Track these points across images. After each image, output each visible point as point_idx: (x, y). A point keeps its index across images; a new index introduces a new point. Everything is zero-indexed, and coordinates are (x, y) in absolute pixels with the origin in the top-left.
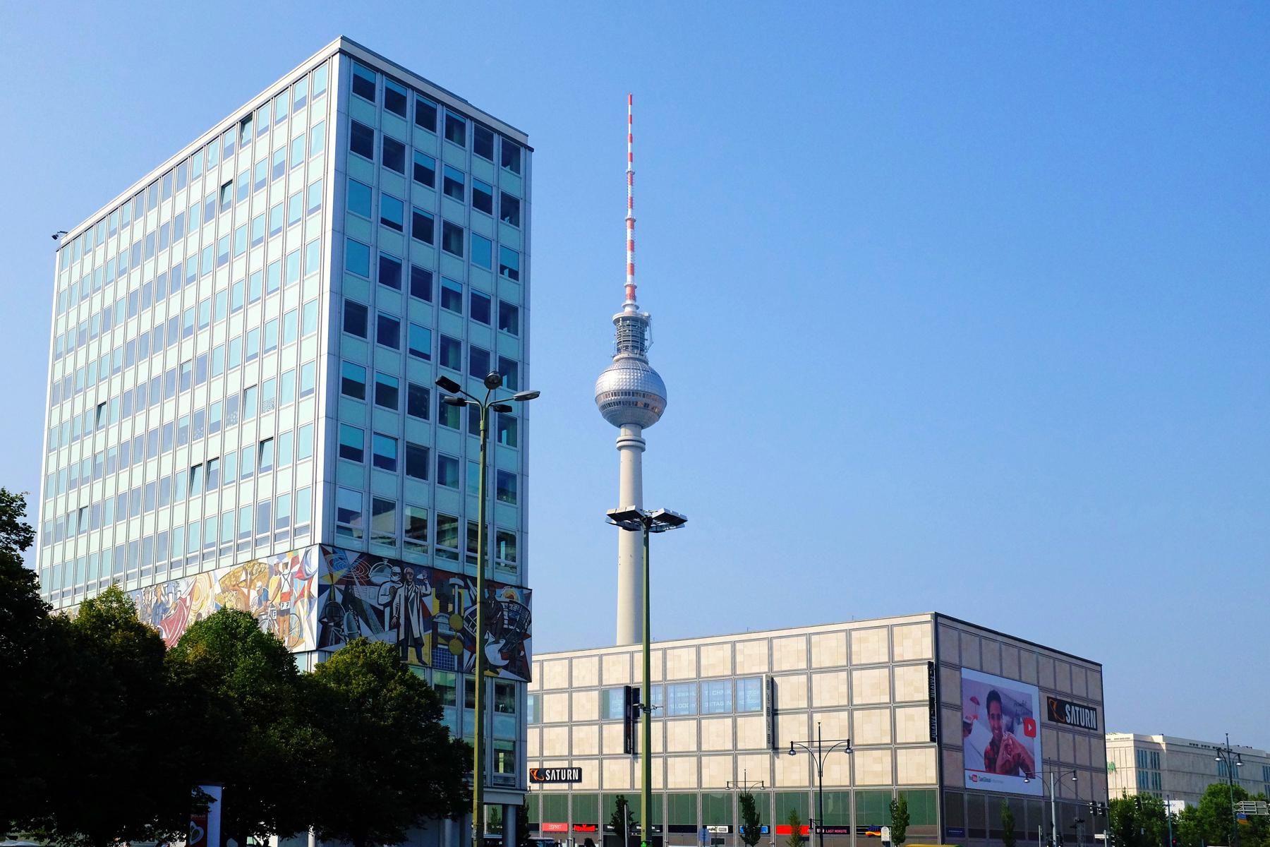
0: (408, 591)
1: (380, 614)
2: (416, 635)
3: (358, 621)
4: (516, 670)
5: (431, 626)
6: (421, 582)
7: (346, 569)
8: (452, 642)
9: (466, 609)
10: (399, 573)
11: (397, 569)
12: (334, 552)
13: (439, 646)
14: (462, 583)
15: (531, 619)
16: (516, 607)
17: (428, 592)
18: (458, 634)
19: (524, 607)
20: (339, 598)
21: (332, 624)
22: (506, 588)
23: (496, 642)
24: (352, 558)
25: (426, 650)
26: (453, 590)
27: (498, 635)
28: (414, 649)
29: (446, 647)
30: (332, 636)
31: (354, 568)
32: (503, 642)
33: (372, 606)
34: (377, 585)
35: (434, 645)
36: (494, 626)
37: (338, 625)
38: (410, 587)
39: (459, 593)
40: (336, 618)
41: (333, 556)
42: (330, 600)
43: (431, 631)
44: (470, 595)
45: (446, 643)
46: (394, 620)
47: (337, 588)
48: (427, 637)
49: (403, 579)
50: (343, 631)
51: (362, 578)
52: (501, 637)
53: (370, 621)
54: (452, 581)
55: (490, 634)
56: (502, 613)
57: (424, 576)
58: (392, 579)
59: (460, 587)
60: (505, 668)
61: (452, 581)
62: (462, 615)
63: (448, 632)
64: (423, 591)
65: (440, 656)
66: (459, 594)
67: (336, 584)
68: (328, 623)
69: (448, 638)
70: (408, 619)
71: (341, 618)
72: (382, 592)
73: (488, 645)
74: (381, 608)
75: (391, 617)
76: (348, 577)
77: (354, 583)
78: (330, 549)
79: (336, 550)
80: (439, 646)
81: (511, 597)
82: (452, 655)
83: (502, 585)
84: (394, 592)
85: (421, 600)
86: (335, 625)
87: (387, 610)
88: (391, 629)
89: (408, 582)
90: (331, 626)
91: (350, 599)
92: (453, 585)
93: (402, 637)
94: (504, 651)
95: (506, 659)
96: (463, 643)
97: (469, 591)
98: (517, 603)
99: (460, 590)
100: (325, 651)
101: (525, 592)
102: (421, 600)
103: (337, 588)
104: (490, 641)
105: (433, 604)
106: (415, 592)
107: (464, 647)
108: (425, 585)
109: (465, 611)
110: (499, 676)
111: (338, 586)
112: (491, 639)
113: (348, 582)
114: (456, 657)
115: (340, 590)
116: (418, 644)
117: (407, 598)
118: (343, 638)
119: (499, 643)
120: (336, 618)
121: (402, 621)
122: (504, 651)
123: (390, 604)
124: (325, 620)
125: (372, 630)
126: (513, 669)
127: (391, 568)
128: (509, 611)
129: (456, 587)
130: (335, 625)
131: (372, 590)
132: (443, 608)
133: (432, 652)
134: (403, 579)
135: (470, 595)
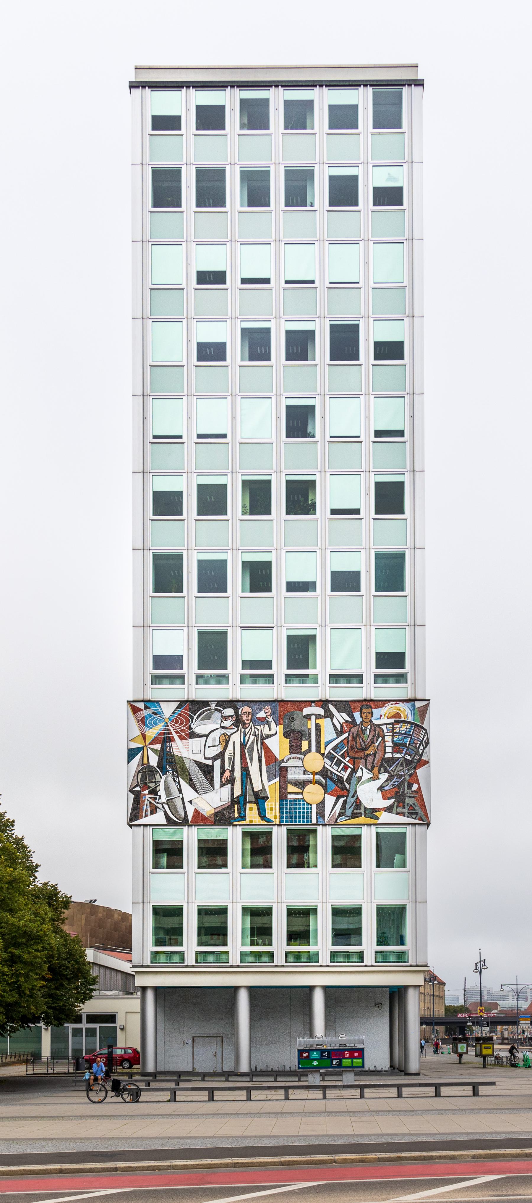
0: (245, 735)
1: (207, 771)
2: (257, 787)
3: (179, 784)
4: (406, 810)
5: (278, 773)
6: (264, 721)
7: (163, 724)
8: (309, 788)
9: (327, 744)
10: (232, 716)
11: (229, 712)
12: (146, 708)
13: (289, 796)
14: (321, 712)
15: (428, 740)
16: (404, 728)
17: (273, 732)
18: (317, 777)
19: (417, 725)
20: (154, 760)
23: (372, 779)
24: (168, 710)
25: (272, 807)
26: (309, 722)
27: (376, 769)
28: (254, 806)
29: (300, 796)
30: (146, 807)
31: (173, 721)
32: (384, 777)
33: (196, 762)
34: (202, 736)
35: (283, 797)
36: (370, 759)
37: (154, 792)
38: (247, 730)
39: (318, 726)
40: (150, 785)
41: (145, 713)
42: (143, 764)
43: (278, 779)
44: (333, 724)
45: (300, 791)
46: (227, 774)
47: (149, 748)
48: (271, 787)
49: (238, 722)
50: (160, 798)
51: (183, 731)
52: (382, 770)
53: (195, 780)
54: (306, 711)
55: (364, 769)
56: (383, 739)
57: (266, 713)
58: (223, 725)
59: (318, 717)
60: (389, 809)
61: (306, 711)
62: (322, 752)
63: (302, 777)
64: (266, 731)
65: (291, 809)
66: (318, 726)
67: (150, 744)
68: (140, 791)
69: (302, 785)
70: (245, 770)
71: (157, 783)
72: (210, 742)
73: (360, 785)
74: (209, 762)
75: (223, 772)
76: (164, 734)
77: (171, 740)
78: (141, 706)
79: (148, 704)
80: (289, 796)
81: (398, 715)
82: (309, 804)
83: (383, 703)
84: (226, 740)
85: (263, 743)
86: (150, 793)
87: (217, 764)
88: (222, 785)
89: (244, 723)
90: (145, 795)
92: (308, 717)
93: (238, 792)
94: (386, 788)
95: (389, 799)
96: (325, 788)
97: (332, 720)
99: (318, 721)
100: (145, 825)
101: (418, 704)
102: (263, 743)
103: (149, 748)
104: (363, 779)
106: (255, 735)
107: (326, 792)
108: (268, 723)
111: (153, 747)
112: (367, 775)
113: (165, 739)
114: (314, 807)
115: (154, 751)
116: (260, 799)
117: (243, 745)
118: (160, 806)
119: (378, 778)
120: (150, 785)
121: (238, 774)
122: (386, 788)
124: (138, 789)
125: (197, 791)
127: (220, 711)
128: (394, 734)
129: (313, 717)
131: (196, 744)
132: (295, 748)
133: (280, 805)
134: (238, 722)
135: (333, 724)
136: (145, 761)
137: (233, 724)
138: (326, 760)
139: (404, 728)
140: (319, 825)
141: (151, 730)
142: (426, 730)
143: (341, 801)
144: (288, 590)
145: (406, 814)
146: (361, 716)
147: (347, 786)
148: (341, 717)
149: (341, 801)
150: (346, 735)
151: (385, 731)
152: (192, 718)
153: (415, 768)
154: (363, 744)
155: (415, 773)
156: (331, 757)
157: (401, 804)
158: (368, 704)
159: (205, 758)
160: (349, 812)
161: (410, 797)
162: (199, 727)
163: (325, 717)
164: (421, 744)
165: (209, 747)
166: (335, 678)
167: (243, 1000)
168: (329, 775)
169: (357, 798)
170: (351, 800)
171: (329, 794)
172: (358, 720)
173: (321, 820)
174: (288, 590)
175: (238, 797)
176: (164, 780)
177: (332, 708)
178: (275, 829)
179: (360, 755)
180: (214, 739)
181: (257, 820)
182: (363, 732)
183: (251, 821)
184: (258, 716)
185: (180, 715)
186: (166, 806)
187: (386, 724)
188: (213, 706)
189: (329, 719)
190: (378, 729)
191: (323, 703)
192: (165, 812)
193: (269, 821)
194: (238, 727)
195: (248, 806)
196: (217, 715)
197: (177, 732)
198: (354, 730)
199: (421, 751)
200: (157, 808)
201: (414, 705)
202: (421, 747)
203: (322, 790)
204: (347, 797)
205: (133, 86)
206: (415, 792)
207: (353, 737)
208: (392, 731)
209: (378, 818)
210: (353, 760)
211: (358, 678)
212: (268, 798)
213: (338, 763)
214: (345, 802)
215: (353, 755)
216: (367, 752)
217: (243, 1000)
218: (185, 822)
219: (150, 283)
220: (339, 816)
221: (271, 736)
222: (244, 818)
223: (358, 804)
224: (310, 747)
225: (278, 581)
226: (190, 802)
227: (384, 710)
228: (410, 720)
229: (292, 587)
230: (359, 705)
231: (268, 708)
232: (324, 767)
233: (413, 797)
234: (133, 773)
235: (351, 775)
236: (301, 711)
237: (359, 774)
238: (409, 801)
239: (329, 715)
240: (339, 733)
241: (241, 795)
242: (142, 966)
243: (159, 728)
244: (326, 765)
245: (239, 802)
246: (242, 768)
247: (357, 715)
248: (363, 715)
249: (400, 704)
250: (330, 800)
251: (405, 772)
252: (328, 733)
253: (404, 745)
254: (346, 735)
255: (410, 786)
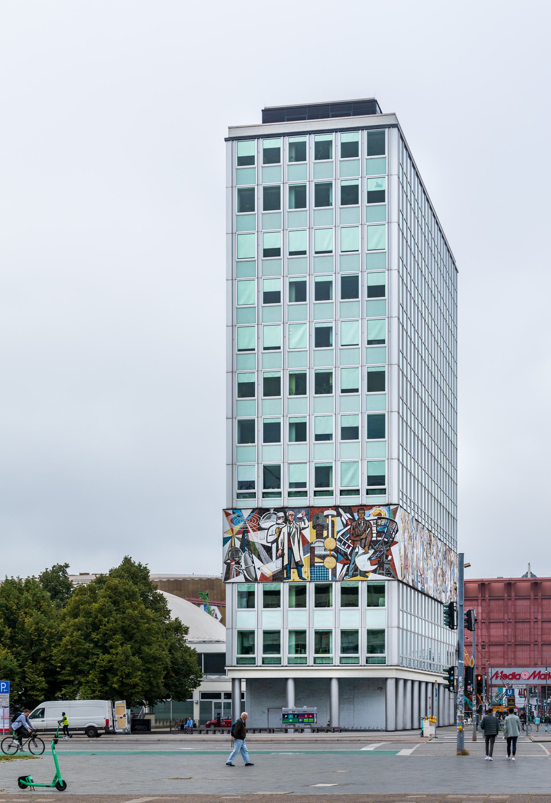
0: (290, 528)
2: (297, 559)
3: (252, 558)
4: (384, 572)
5: (309, 550)
6: (301, 519)
7: (243, 523)
8: (327, 559)
9: (338, 532)
10: (283, 517)
11: (281, 514)
12: (234, 513)
13: (316, 564)
14: (334, 513)
15: (398, 529)
16: (383, 522)
17: (306, 526)
18: (332, 552)
19: (391, 520)
20: (238, 544)
21: (234, 563)
22: (374, 508)
23: (364, 553)
24: (246, 514)
25: (306, 571)
26: (328, 519)
27: (367, 547)
28: (295, 570)
29: (322, 564)
30: (233, 572)
31: (249, 521)
32: (371, 552)
33: (262, 544)
34: (266, 529)
35: (312, 565)
36: (363, 541)
37: (238, 563)
38: (291, 525)
39: (333, 522)
40: (236, 559)
41: (233, 516)
43: (309, 554)
44: (342, 520)
46: (280, 552)
48: (305, 559)
49: (286, 520)
50: (241, 567)
51: (254, 526)
52: (370, 547)
53: (261, 556)
55: (360, 547)
56: (371, 528)
57: (302, 514)
58: (277, 522)
59: (333, 516)
60: (374, 571)
61: (326, 513)
63: (324, 553)
64: (303, 525)
65: (317, 572)
66: (333, 522)
67: (236, 535)
68: (230, 563)
69: (323, 557)
70: (290, 549)
71: (240, 558)
72: (270, 533)
73: (358, 556)
74: (269, 545)
75: (277, 550)
76: (244, 528)
77: (248, 532)
78: (230, 512)
79: (235, 511)
80: (316, 564)
81: (380, 514)
82: (327, 569)
83: (371, 507)
84: (280, 531)
85: (300, 533)
86: (236, 563)
87: (274, 546)
88: (277, 558)
89: (290, 521)
90: (233, 565)
91: (247, 545)
92: (327, 516)
93: (286, 562)
94: (373, 559)
95: (374, 565)
97: (341, 518)
98: (384, 518)
99: (333, 519)
100: (233, 583)
102: (300, 533)
105: (309, 534)
106: (296, 528)
107: (337, 561)
108: (304, 521)
109: (337, 534)
110: (368, 579)
111: (237, 536)
112: (361, 551)
113: (245, 531)
114: (330, 570)
115: (238, 538)
116: (299, 566)
117: (289, 534)
118: (241, 571)
119: (368, 553)
120: (236, 559)
121: (286, 551)
122: (373, 559)
123: (276, 541)
124: (229, 561)
125: (262, 562)
126: (381, 571)
127: (276, 514)
128: (377, 526)
129: (330, 517)
130: (236, 563)
132: (319, 535)
133: (310, 570)
134: (286, 520)
135: (342, 520)
136: (233, 545)
137: (283, 522)
138: (338, 542)
139: (383, 522)
140: (334, 581)
141: (236, 526)
142: (396, 523)
143: (346, 566)
144: (316, 440)
145: (385, 574)
146: (358, 515)
147: (350, 558)
148: (346, 516)
149: (346, 566)
150: (349, 527)
151: (372, 524)
152: (260, 519)
153: (390, 546)
154: (359, 532)
155: (390, 549)
156: (340, 540)
157: (381, 568)
158: (363, 508)
159: (267, 542)
160: (350, 573)
161: (387, 564)
162: (264, 524)
163: (337, 516)
164: (394, 531)
165: (270, 536)
166: (342, 492)
167: (291, 686)
168: (339, 551)
169: (356, 564)
170: (352, 566)
171: (339, 563)
172: (357, 517)
173: (334, 578)
174: (316, 440)
175: (286, 565)
176: (244, 556)
177: (341, 511)
178: (308, 584)
179: (356, 539)
180: (273, 531)
181: (297, 578)
182: (359, 524)
183: (294, 579)
184: (298, 516)
185: (253, 517)
186: (245, 571)
187: (373, 520)
188: (272, 511)
189: (339, 517)
190: (368, 523)
191: (336, 508)
192: (244, 575)
193: (304, 579)
194: (286, 523)
195: (292, 570)
196: (274, 516)
197: (251, 527)
198: (354, 524)
199: (393, 536)
200: (240, 572)
201: (389, 508)
202: (394, 533)
203: (334, 560)
204: (350, 564)
205: (227, 140)
206: (390, 560)
207: (353, 528)
208: (376, 524)
209: (367, 577)
210: (353, 542)
211: (357, 492)
212: (303, 565)
213: (345, 544)
214: (348, 567)
215: (353, 539)
216: (362, 537)
217: (291, 686)
218: (256, 580)
219: (237, 258)
220: (346, 575)
221: (305, 528)
222: (289, 577)
223: (356, 569)
224: (328, 535)
225: (310, 434)
226: (259, 569)
227: (372, 511)
228: (387, 517)
229: (319, 437)
230: (357, 508)
231: (303, 512)
232: (336, 547)
233: (389, 564)
234: (226, 552)
235: (352, 551)
236: (323, 513)
237: (357, 550)
238: (386, 566)
239: (339, 515)
240: (345, 526)
241: (288, 564)
242: (232, 666)
243: (241, 525)
244: (337, 545)
245: (286, 568)
246: (288, 548)
247: (356, 515)
248: (360, 515)
249: (382, 507)
250: (339, 566)
251: (384, 548)
252: (339, 526)
253: (383, 532)
254: (349, 527)
255: (387, 557)
